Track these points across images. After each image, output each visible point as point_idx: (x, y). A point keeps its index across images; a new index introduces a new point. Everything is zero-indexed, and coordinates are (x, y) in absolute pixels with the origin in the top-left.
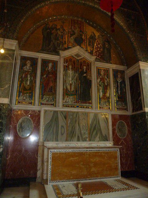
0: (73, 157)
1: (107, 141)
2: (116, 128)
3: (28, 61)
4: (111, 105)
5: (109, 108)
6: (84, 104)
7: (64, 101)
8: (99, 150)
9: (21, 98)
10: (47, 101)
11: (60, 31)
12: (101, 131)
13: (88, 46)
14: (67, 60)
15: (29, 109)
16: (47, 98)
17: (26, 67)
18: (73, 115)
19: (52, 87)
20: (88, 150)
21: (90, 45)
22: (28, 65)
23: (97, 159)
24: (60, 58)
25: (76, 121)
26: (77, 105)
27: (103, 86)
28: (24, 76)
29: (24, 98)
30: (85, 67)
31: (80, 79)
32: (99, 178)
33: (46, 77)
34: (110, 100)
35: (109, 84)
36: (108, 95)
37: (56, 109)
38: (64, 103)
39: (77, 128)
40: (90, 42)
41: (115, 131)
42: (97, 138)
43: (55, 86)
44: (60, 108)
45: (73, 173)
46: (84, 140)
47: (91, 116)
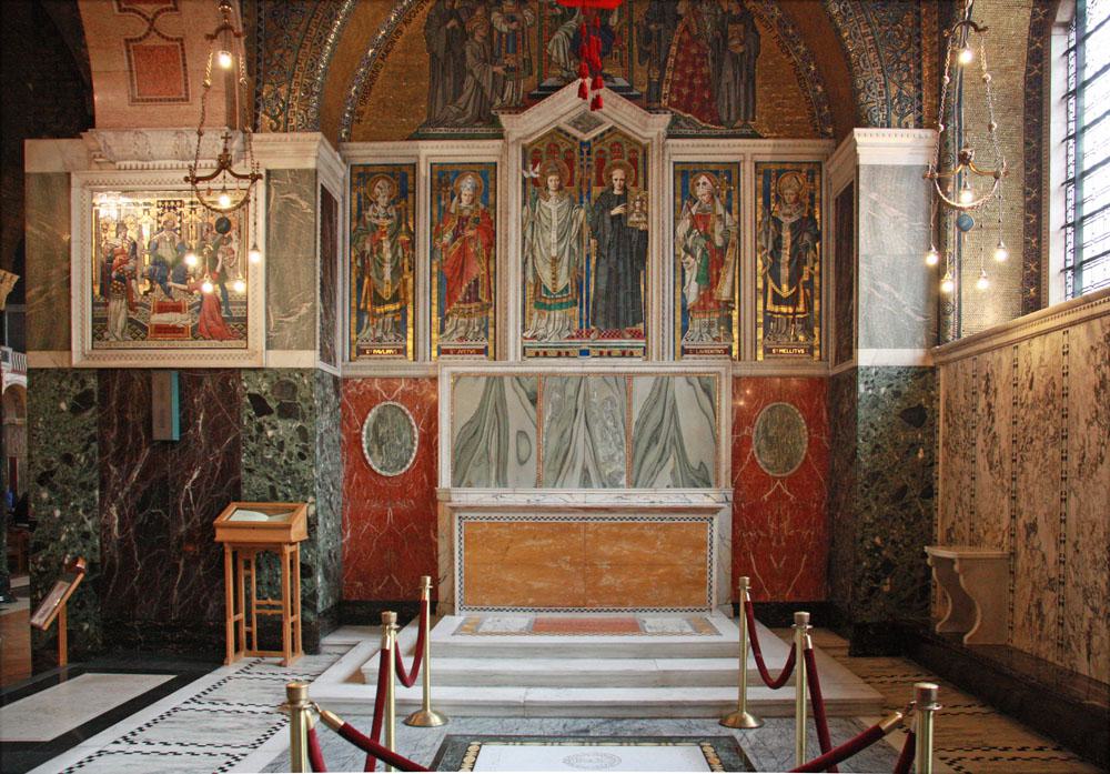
0: (534, 538)
1: (709, 485)
2: (754, 436)
3: (379, 183)
4: (736, 336)
5: (728, 351)
6: (614, 342)
7: (528, 334)
8: (633, 516)
9: (367, 333)
10: (461, 339)
11: (501, 12)
12: (683, 448)
13: (636, 58)
14: (536, 151)
16: (462, 328)
17: (374, 210)
18: (563, 391)
19: (476, 281)
20: (592, 516)
22: (383, 201)
23: (625, 548)
24: (505, 150)
25: (576, 411)
26: (585, 347)
27: (703, 251)
28: (368, 248)
29: (378, 334)
30: (618, 174)
31: (594, 233)
32: (629, 609)
33: (454, 240)
34: (735, 313)
35: (733, 241)
36: (724, 291)
40: (647, 38)
41: (749, 444)
42: (665, 475)
43: (488, 272)
44: (513, 362)
45: (536, 587)
46: (610, 482)
47: (642, 388)
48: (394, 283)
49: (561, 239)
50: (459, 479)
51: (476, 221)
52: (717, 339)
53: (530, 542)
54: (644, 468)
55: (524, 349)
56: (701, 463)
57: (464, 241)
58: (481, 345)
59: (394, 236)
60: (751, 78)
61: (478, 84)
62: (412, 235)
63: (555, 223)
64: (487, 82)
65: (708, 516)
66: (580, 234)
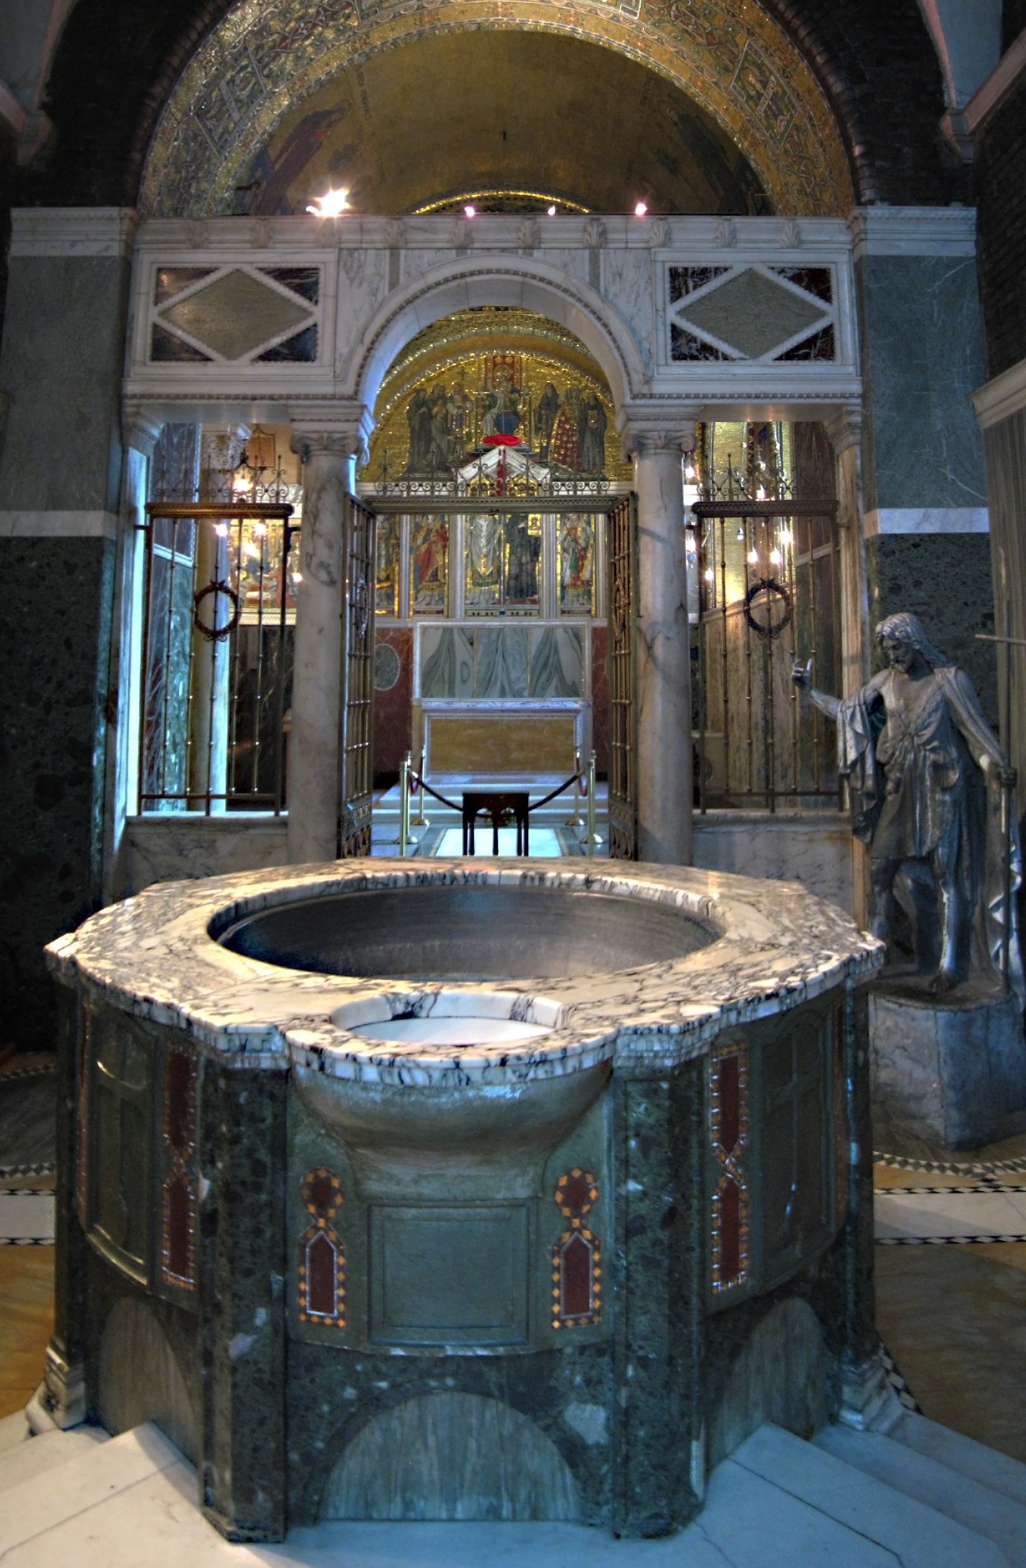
5: (589, 612)
6: (520, 606)
7: (468, 602)
10: (427, 604)
12: (561, 671)
15: (388, 626)
16: (428, 598)
18: (489, 637)
21: (540, 429)
33: (423, 543)
36: (585, 575)
37: (449, 623)
38: (469, 607)
39: (499, 669)
42: (551, 689)
46: (517, 694)
47: (537, 637)
48: (386, 570)
49: (489, 542)
50: (426, 692)
51: (437, 531)
52: (583, 604)
53: (470, 732)
54: (539, 684)
55: (466, 611)
56: (574, 682)
57: (430, 545)
58: (439, 608)
59: (387, 540)
60: (602, 444)
61: (439, 446)
62: (398, 539)
63: (484, 533)
64: (444, 446)
65: (573, 714)
66: (499, 540)
